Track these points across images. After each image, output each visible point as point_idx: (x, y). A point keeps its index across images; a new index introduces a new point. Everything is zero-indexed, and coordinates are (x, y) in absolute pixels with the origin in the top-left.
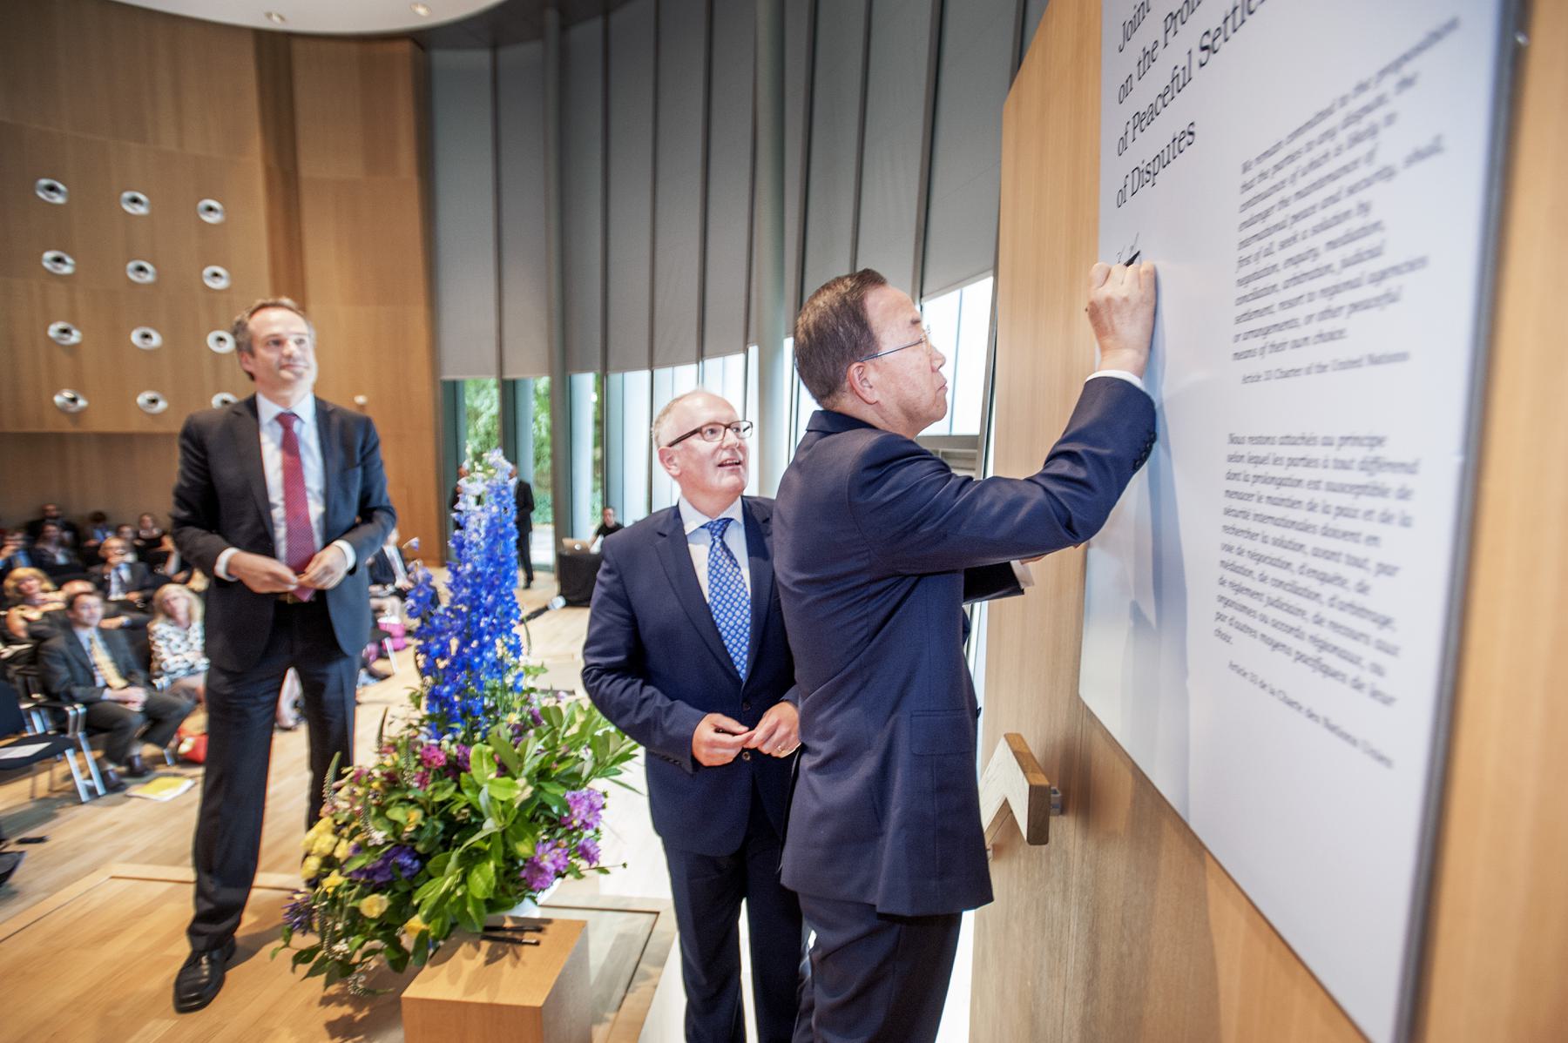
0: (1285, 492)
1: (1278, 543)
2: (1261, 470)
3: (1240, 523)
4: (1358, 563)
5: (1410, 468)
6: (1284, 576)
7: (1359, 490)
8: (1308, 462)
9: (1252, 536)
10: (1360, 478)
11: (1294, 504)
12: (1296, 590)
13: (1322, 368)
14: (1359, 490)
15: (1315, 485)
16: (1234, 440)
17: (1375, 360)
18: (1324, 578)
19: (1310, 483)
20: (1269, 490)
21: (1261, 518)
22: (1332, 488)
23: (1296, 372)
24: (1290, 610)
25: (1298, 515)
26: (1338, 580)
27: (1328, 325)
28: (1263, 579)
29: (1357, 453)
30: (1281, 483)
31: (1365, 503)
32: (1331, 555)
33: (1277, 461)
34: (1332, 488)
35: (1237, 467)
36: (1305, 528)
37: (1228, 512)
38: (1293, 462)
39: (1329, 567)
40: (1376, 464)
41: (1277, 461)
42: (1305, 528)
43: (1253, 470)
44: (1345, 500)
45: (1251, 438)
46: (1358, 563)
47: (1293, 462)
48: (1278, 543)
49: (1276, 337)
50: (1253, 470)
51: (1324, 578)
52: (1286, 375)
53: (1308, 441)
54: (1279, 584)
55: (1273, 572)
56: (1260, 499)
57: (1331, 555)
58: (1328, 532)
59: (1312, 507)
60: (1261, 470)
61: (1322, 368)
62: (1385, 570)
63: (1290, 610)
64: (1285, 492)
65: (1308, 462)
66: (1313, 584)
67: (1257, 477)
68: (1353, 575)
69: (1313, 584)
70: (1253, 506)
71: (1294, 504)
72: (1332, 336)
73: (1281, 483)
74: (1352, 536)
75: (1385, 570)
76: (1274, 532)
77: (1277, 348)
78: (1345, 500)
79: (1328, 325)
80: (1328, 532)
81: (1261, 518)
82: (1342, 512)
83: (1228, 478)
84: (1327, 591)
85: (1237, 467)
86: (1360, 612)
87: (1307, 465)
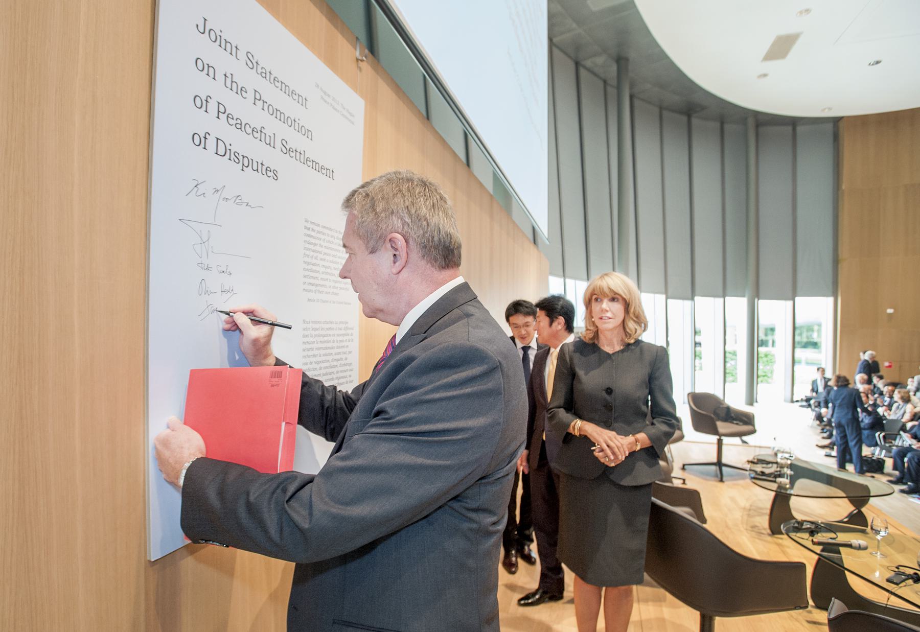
0: (326, 339)
1: (325, 355)
2: (317, 332)
3: (310, 353)
4: (345, 353)
5: (352, 329)
6: (327, 364)
7: (344, 335)
8: (331, 329)
9: (315, 356)
10: (343, 332)
11: (328, 342)
12: (331, 367)
13: (334, 302)
14: (344, 335)
15: (334, 335)
16: (305, 322)
17: (346, 304)
18: (338, 360)
19: (333, 335)
20: (321, 339)
21: (318, 349)
22: (338, 335)
23: (327, 301)
24: (330, 374)
25: (330, 345)
26: (342, 359)
27: (335, 291)
28: (321, 369)
29: (343, 326)
30: (324, 336)
31: (346, 338)
32: (339, 353)
33: (322, 329)
34: (338, 335)
35: (306, 333)
36: (332, 348)
37: (304, 350)
38: (327, 329)
39: (338, 357)
40: (346, 328)
41: (322, 329)
42: (332, 348)
43: (314, 333)
44: (341, 338)
45: (313, 322)
46: (345, 353)
47: (327, 329)
48: (325, 355)
49: (321, 289)
50: (314, 333)
51: (338, 360)
52: (324, 302)
53: (331, 323)
54: (327, 367)
55: (323, 365)
56: (317, 343)
57: (339, 353)
58: (338, 347)
59: (334, 342)
60: (317, 332)
61: (334, 302)
62: (350, 352)
63: (330, 374)
64: (326, 339)
65: (331, 329)
66: (335, 363)
67: (316, 335)
68: (343, 356)
69: (335, 363)
70: (315, 346)
71: (328, 342)
72: (336, 294)
73: (324, 336)
74: (343, 347)
75: (350, 352)
76: (322, 352)
77: (321, 292)
78: (341, 338)
79: (335, 291)
80: (338, 347)
81: (318, 349)
82: (341, 341)
83: (304, 337)
84: (338, 363)
85: (306, 333)
86: (345, 365)
87: (332, 330)
